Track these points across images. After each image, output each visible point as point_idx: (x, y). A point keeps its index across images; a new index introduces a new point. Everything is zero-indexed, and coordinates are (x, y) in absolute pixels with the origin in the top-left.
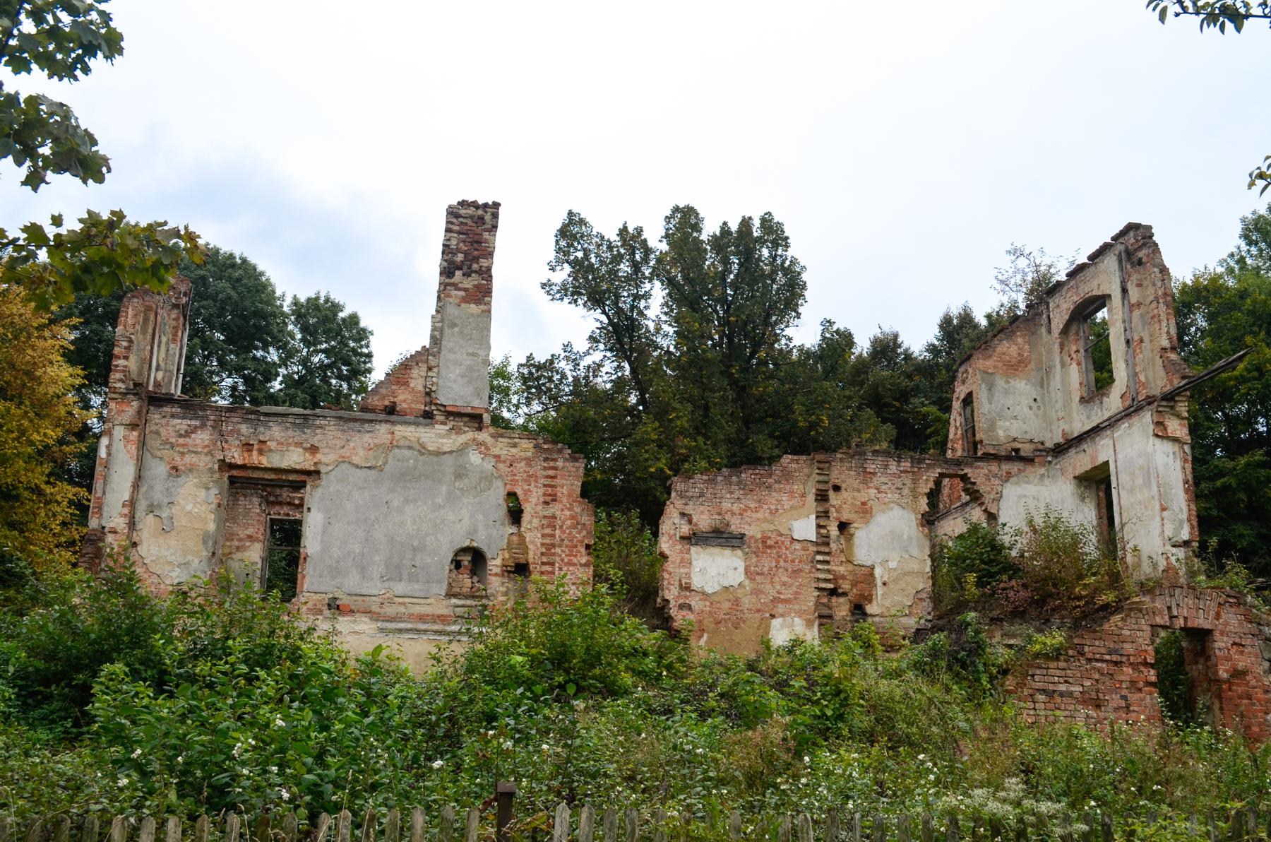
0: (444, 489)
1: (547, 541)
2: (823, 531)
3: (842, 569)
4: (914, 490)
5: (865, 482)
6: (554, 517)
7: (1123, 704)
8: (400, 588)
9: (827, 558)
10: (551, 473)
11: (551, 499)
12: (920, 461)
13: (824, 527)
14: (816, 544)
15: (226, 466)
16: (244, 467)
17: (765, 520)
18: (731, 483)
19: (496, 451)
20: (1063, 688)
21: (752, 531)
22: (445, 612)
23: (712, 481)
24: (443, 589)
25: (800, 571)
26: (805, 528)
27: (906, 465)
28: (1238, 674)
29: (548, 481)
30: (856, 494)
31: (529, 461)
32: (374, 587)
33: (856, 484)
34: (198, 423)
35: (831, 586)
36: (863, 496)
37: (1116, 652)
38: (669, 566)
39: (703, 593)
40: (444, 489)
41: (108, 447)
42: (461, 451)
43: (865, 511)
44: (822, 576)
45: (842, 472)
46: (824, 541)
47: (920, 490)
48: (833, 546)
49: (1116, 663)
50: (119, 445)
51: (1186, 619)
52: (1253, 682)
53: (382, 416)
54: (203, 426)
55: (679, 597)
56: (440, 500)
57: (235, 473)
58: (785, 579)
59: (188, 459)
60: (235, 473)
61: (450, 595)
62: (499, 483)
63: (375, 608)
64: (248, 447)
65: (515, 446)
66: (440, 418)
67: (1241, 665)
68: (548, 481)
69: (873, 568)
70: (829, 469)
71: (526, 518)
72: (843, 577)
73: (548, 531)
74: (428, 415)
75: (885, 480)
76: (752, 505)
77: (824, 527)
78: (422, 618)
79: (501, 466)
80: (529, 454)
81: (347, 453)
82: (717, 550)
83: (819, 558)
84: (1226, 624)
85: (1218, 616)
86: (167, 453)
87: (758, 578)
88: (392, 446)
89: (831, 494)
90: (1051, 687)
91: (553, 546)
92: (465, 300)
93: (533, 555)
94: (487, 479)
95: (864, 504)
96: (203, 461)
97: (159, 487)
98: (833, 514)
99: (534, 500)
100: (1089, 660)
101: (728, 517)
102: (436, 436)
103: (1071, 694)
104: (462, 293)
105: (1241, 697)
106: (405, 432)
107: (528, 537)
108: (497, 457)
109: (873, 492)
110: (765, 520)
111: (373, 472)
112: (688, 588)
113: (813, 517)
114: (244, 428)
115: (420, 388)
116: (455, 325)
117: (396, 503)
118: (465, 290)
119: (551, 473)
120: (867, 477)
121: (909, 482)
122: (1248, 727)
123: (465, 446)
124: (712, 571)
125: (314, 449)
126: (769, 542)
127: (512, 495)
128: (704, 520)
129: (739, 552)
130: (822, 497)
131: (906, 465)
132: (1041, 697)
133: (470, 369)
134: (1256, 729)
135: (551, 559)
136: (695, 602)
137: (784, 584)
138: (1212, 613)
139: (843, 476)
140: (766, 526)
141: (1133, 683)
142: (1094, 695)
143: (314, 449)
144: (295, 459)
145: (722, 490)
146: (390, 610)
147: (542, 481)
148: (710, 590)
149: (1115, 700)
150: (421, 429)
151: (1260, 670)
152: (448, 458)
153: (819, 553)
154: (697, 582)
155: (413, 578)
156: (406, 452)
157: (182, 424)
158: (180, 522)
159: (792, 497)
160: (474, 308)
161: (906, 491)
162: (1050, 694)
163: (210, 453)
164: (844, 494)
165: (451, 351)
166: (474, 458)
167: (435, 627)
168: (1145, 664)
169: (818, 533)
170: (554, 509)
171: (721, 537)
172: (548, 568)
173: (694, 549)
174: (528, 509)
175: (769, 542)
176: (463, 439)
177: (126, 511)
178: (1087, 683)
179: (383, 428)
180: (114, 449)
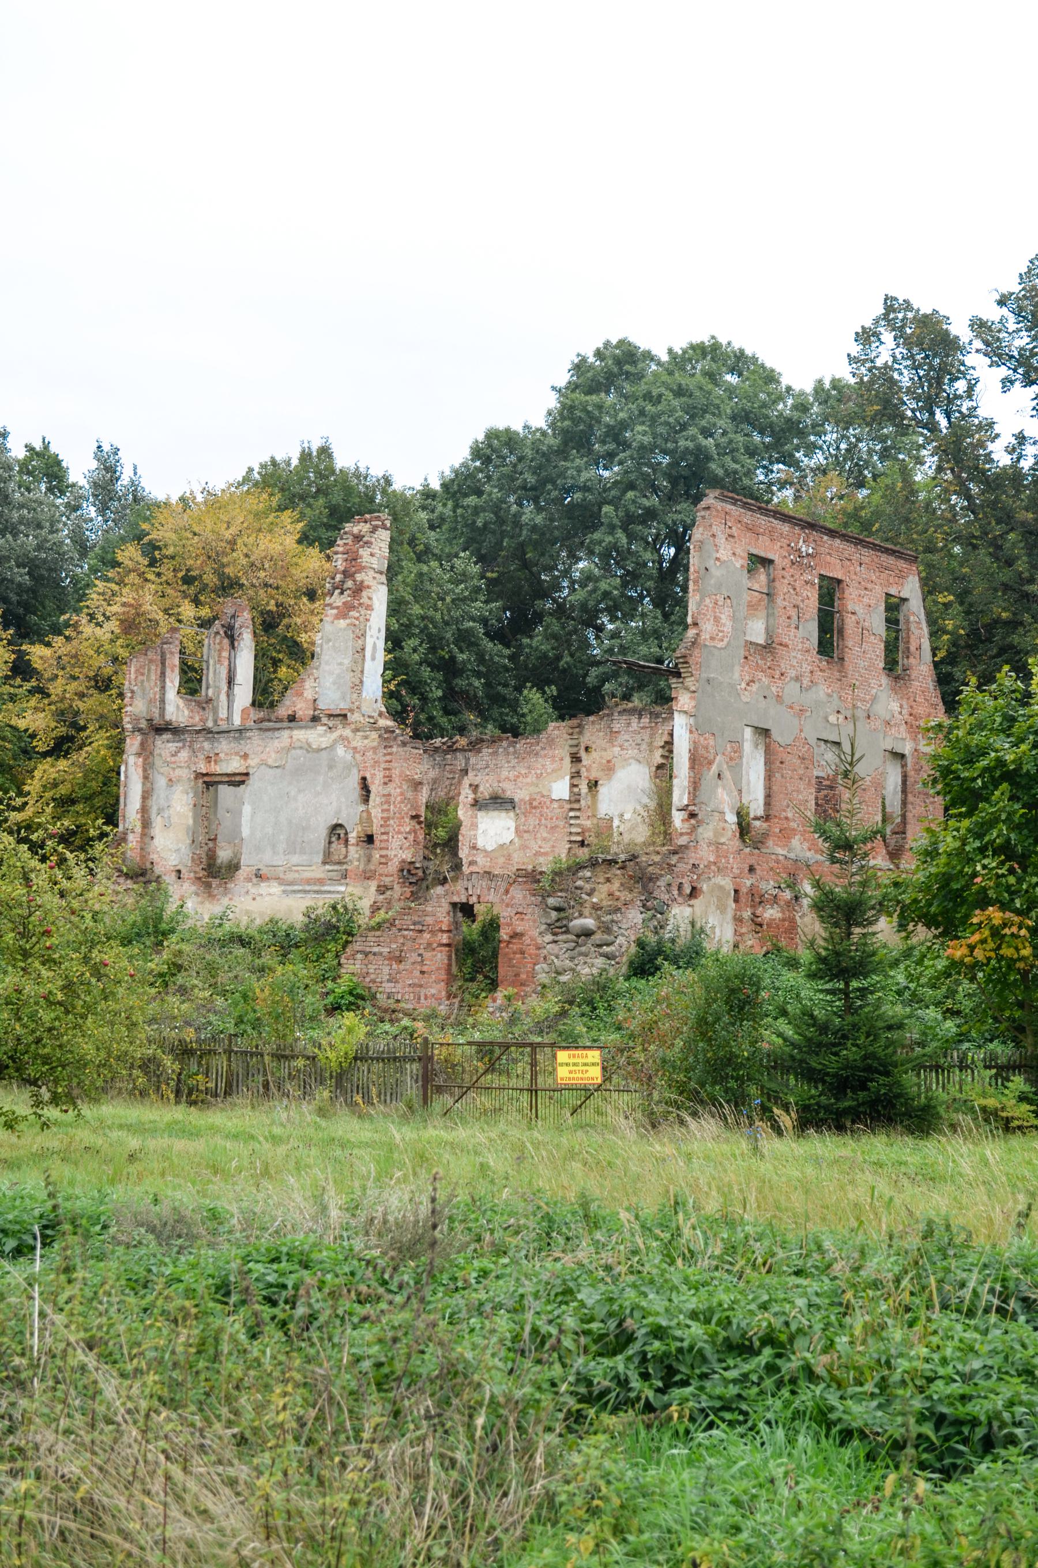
0: (321, 779)
1: (385, 815)
2: (576, 790)
3: (588, 823)
4: (650, 744)
5: (611, 741)
6: (389, 795)
7: (419, 959)
8: (295, 859)
9: (578, 814)
10: (388, 758)
11: (388, 780)
12: (657, 715)
13: (576, 786)
14: (570, 801)
15: (199, 775)
16: (207, 774)
17: (532, 784)
18: (508, 754)
19: (354, 744)
20: (376, 949)
21: (520, 795)
22: (322, 876)
23: (495, 753)
24: (319, 858)
25: (557, 826)
26: (561, 789)
27: (645, 720)
28: (515, 935)
29: (386, 765)
30: (604, 753)
31: (375, 749)
32: (279, 860)
33: (603, 743)
34: (180, 744)
35: (579, 838)
36: (608, 755)
37: (419, 923)
38: (463, 830)
39: (485, 851)
40: (321, 779)
41: (126, 771)
42: (331, 748)
43: (609, 768)
44: (574, 830)
45: (593, 731)
46: (575, 798)
47: (655, 744)
48: (583, 802)
49: (421, 931)
50: (132, 769)
51: (479, 897)
52: (528, 941)
53: (286, 724)
54: (184, 746)
55: (468, 855)
56: (319, 788)
57: (206, 779)
58: (545, 835)
59: (178, 772)
60: (206, 779)
61: (324, 863)
62: (355, 771)
63: (282, 876)
64: (208, 759)
65: (366, 737)
66: (325, 720)
67: (519, 929)
68: (386, 765)
69: (611, 819)
70: (580, 733)
71: (372, 796)
72: (589, 830)
73: (385, 807)
74: (315, 719)
75: (626, 737)
76: (523, 772)
77: (576, 786)
78: (308, 882)
79: (357, 756)
80: (375, 744)
81: (264, 756)
82: (496, 813)
83: (572, 814)
84: (513, 898)
85: (507, 892)
86: (165, 770)
87: (526, 835)
88: (291, 747)
89: (583, 754)
90: (368, 949)
91: (388, 818)
92: (337, 617)
93: (376, 829)
94: (348, 768)
95: (609, 762)
96: (185, 774)
97: (162, 795)
98: (584, 773)
99: (377, 782)
100: (400, 930)
101: (505, 785)
102: (317, 736)
103: (381, 954)
104: (335, 611)
105: (515, 953)
106: (299, 735)
107: (373, 812)
108: (355, 748)
109: (617, 749)
110: (532, 784)
111: (279, 771)
112: (474, 847)
113: (568, 778)
114: (206, 745)
115: (310, 697)
116: (330, 640)
117: (293, 793)
118: (337, 608)
119: (388, 758)
120: (613, 734)
121: (647, 738)
122: (517, 975)
123: (335, 741)
124: (491, 832)
125: (245, 756)
126: (535, 804)
127: (364, 779)
128: (485, 791)
129: (512, 814)
130: (576, 759)
131: (645, 720)
132: (359, 956)
133: (339, 676)
134: (523, 976)
135: (387, 829)
136: (480, 860)
137: (544, 839)
138: (502, 890)
139: (593, 738)
140: (533, 789)
141: (429, 944)
142: (397, 954)
143: (245, 756)
144: (234, 765)
145: (501, 759)
146: (290, 876)
147: (383, 766)
148: (489, 848)
149: (414, 957)
150: (309, 732)
151: (535, 933)
152: (324, 754)
153: (572, 810)
154: (480, 844)
155: (303, 852)
156: (299, 752)
157: (172, 746)
158: (175, 820)
159: (554, 761)
160: (342, 623)
161: (644, 746)
162: (366, 954)
163: (188, 767)
164: (594, 755)
165: (327, 663)
166: (340, 751)
167: (316, 888)
168: (443, 931)
169: (571, 792)
170: (391, 788)
171: (499, 802)
172: (385, 837)
173: (480, 814)
174: (373, 788)
175: (535, 804)
176: (335, 735)
177: (139, 816)
178: (394, 946)
179: (286, 733)
180: (129, 774)
